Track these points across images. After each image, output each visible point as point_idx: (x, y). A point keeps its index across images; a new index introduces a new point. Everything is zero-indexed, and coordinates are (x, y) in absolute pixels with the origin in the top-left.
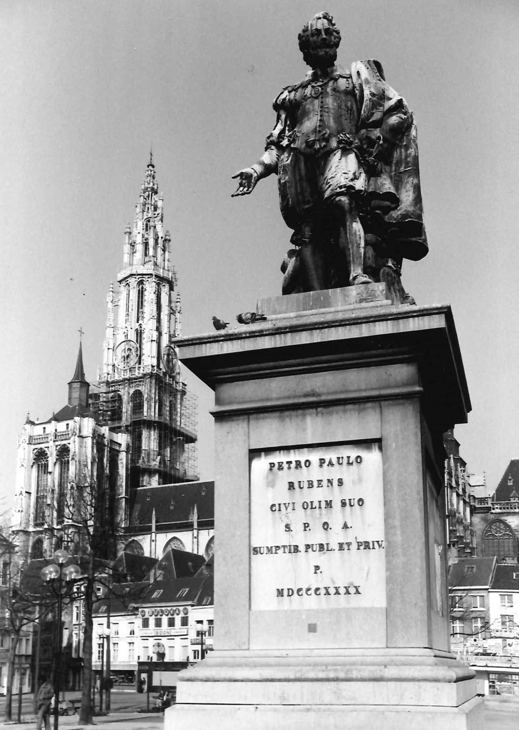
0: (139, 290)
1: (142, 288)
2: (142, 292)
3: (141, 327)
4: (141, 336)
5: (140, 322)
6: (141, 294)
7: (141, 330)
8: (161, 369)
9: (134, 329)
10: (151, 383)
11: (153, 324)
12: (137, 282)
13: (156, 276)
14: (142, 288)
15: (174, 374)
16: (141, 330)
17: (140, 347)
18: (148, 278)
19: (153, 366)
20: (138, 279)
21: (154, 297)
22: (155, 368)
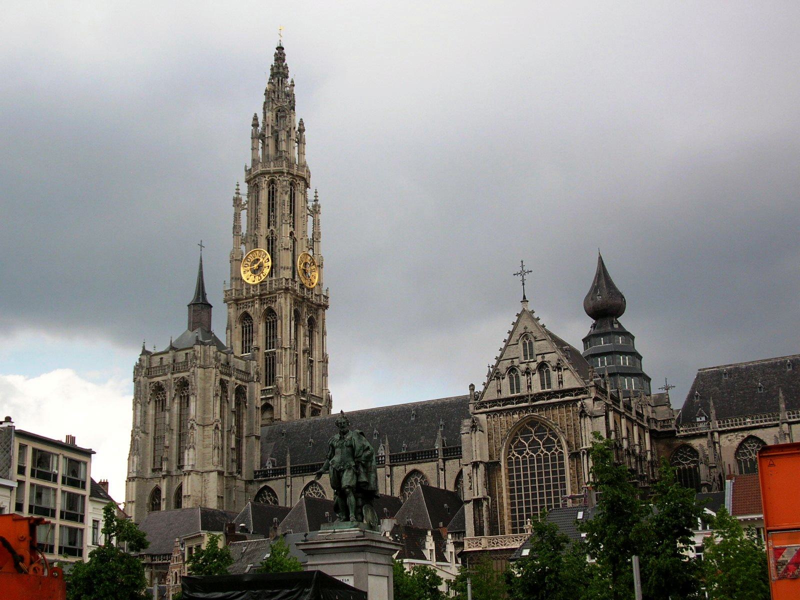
0: (269, 192)
1: (273, 188)
2: (273, 192)
3: (272, 234)
4: (272, 244)
5: (272, 228)
6: (272, 195)
7: (272, 237)
8: (296, 282)
9: (264, 237)
10: (286, 299)
11: (286, 229)
12: (266, 182)
13: (287, 173)
14: (273, 188)
15: (312, 286)
16: (272, 237)
17: (272, 257)
18: (280, 176)
19: (287, 280)
20: (267, 178)
21: (287, 198)
22: (290, 280)
